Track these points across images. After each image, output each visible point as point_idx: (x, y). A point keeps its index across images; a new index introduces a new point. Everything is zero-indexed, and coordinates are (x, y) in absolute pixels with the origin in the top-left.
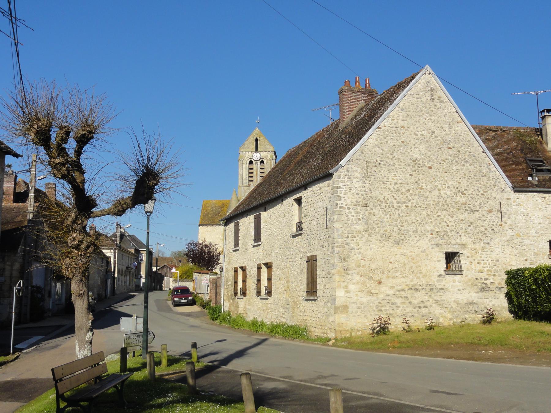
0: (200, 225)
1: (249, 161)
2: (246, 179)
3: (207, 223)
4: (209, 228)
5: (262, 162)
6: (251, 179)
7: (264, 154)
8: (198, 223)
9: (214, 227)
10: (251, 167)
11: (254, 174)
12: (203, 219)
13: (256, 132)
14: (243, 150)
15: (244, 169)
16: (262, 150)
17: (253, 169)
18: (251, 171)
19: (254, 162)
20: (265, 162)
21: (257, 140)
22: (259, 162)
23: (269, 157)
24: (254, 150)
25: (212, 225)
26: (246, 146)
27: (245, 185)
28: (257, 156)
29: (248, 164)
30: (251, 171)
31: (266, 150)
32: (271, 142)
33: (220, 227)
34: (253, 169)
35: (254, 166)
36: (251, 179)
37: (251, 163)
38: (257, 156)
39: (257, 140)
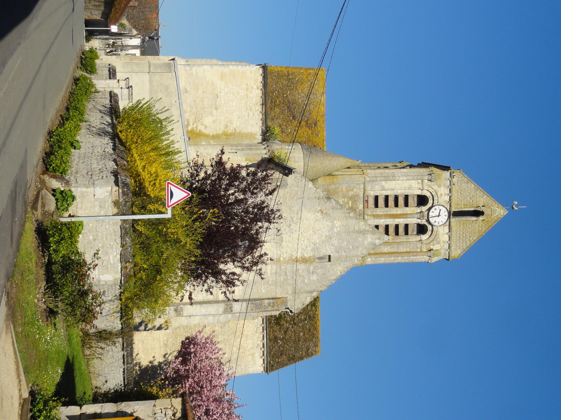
0: (264, 68)
1: (428, 194)
2: (383, 189)
3: (270, 88)
4: (257, 94)
5: (422, 229)
6: (381, 202)
7: (443, 233)
8: (273, 66)
9: (259, 108)
10: (413, 201)
11: (393, 210)
12: (280, 75)
13: (497, 211)
14: (455, 180)
15: (407, 184)
16: (454, 228)
17: (406, 205)
18: (401, 201)
19: (424, 209)
20: (424, 237)
21: (477, 213)
22: (424, 222)
23: (435, 247)
24: (453, 210)
25: (264, 104)
26: (464, 186)
27: (368, 187)
28: (439, 216)
29: (419, 192)
30: (401, 201)
31: (453, 238)
32: (472, 252)
33: (260, 123)
34: (406, 205)
35: (413, 209)
36: (381, 202)
37: (422, 200)
38: (439, 216)
39: (477, 213)
